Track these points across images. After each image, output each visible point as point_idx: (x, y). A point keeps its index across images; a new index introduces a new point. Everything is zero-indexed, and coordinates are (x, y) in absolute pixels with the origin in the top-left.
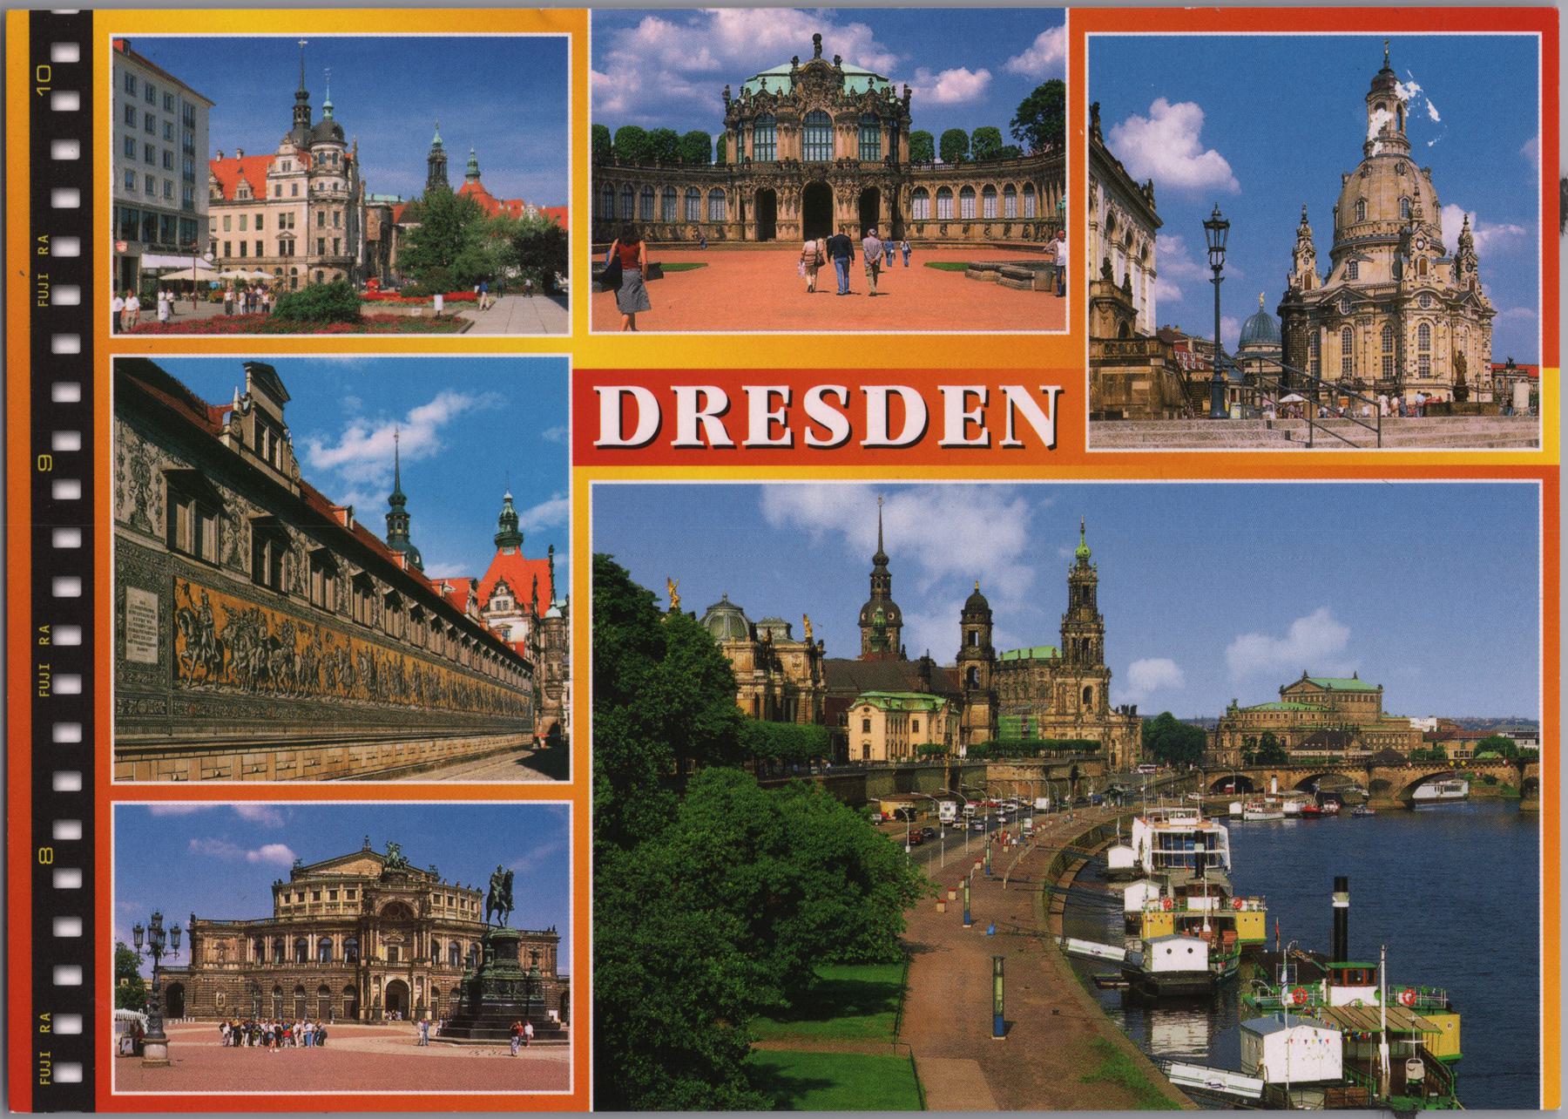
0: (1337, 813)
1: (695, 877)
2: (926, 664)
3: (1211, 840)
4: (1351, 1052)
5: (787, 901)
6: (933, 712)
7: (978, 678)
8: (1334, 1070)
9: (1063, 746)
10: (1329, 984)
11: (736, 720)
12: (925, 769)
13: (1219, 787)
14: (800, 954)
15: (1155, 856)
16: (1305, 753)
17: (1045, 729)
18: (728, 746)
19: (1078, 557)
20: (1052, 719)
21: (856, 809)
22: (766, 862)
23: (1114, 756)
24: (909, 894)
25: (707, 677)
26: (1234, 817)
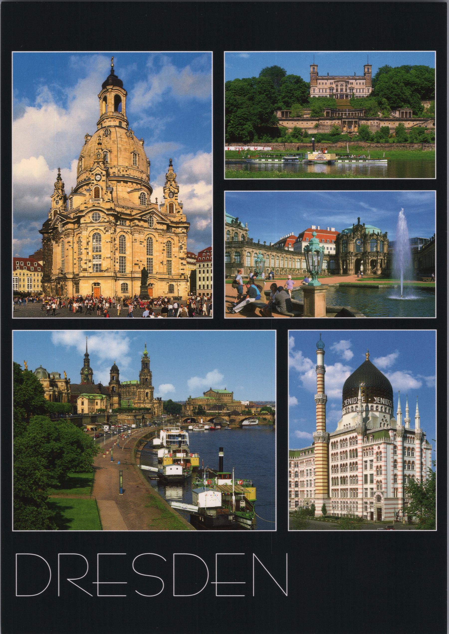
0: (220, 429)
1: (32, 447)
2: (100, 385)
3: (183, 436)
4: (224, 499)
5: (59, 454)
6: (102, 400)
7: (116, 389)
8: (218, 503)
9: (140, 409)
10: (218, 479)
11: (44, 401)
12: (100, 416)
13: (186, 421)
14: (63, 470)
15: (167, 441)
16: (211, 411)
17: (134, 404)
18: (42, 409)
19: (144, 354)
20: (137, 401)
21: (80, 427)
22: (53, 443)
23: (155, 412)
24: (95, 452)
25: (35, 389)
26: (190, 430)
